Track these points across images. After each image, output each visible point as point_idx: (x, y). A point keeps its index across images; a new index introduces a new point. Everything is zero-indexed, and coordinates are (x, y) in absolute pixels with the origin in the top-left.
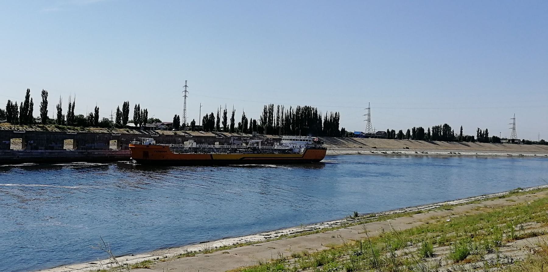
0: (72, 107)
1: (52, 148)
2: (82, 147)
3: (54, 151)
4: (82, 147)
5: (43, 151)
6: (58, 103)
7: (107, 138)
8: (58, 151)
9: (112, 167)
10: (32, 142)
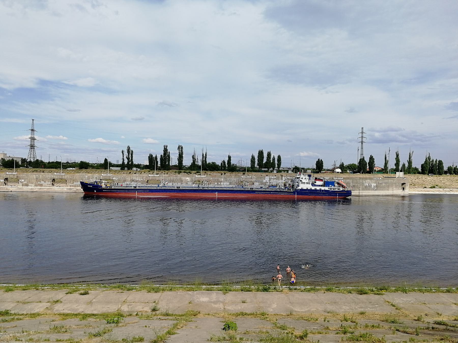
0: (205, 157)
1: (41, 185)
2: (70, 184)
3: (42, 187)
4: (70, 184)
5: (32, 187)
6: (193, 154)
8: (47, 187)
9: (103, 200)
10: (23, 180)
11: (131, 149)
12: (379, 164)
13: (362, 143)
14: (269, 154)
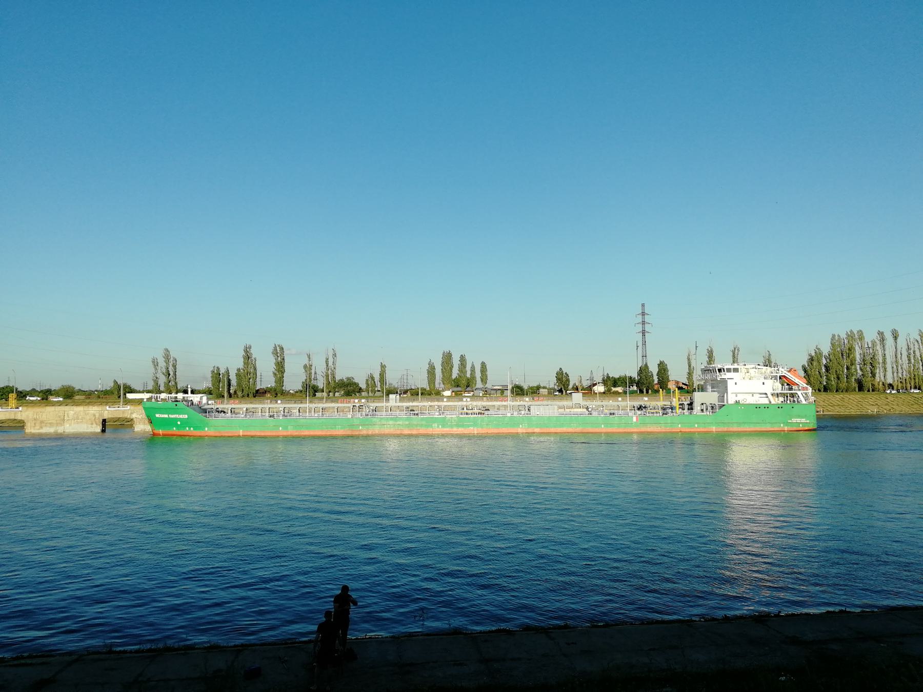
7: (94, 415)
11: (173, 354)
12: (677, 374)
13: (644, 335)
14: (463, 359)
